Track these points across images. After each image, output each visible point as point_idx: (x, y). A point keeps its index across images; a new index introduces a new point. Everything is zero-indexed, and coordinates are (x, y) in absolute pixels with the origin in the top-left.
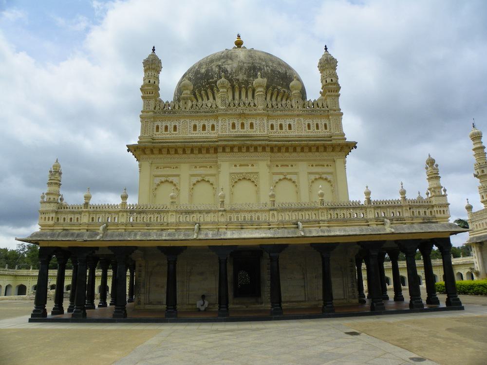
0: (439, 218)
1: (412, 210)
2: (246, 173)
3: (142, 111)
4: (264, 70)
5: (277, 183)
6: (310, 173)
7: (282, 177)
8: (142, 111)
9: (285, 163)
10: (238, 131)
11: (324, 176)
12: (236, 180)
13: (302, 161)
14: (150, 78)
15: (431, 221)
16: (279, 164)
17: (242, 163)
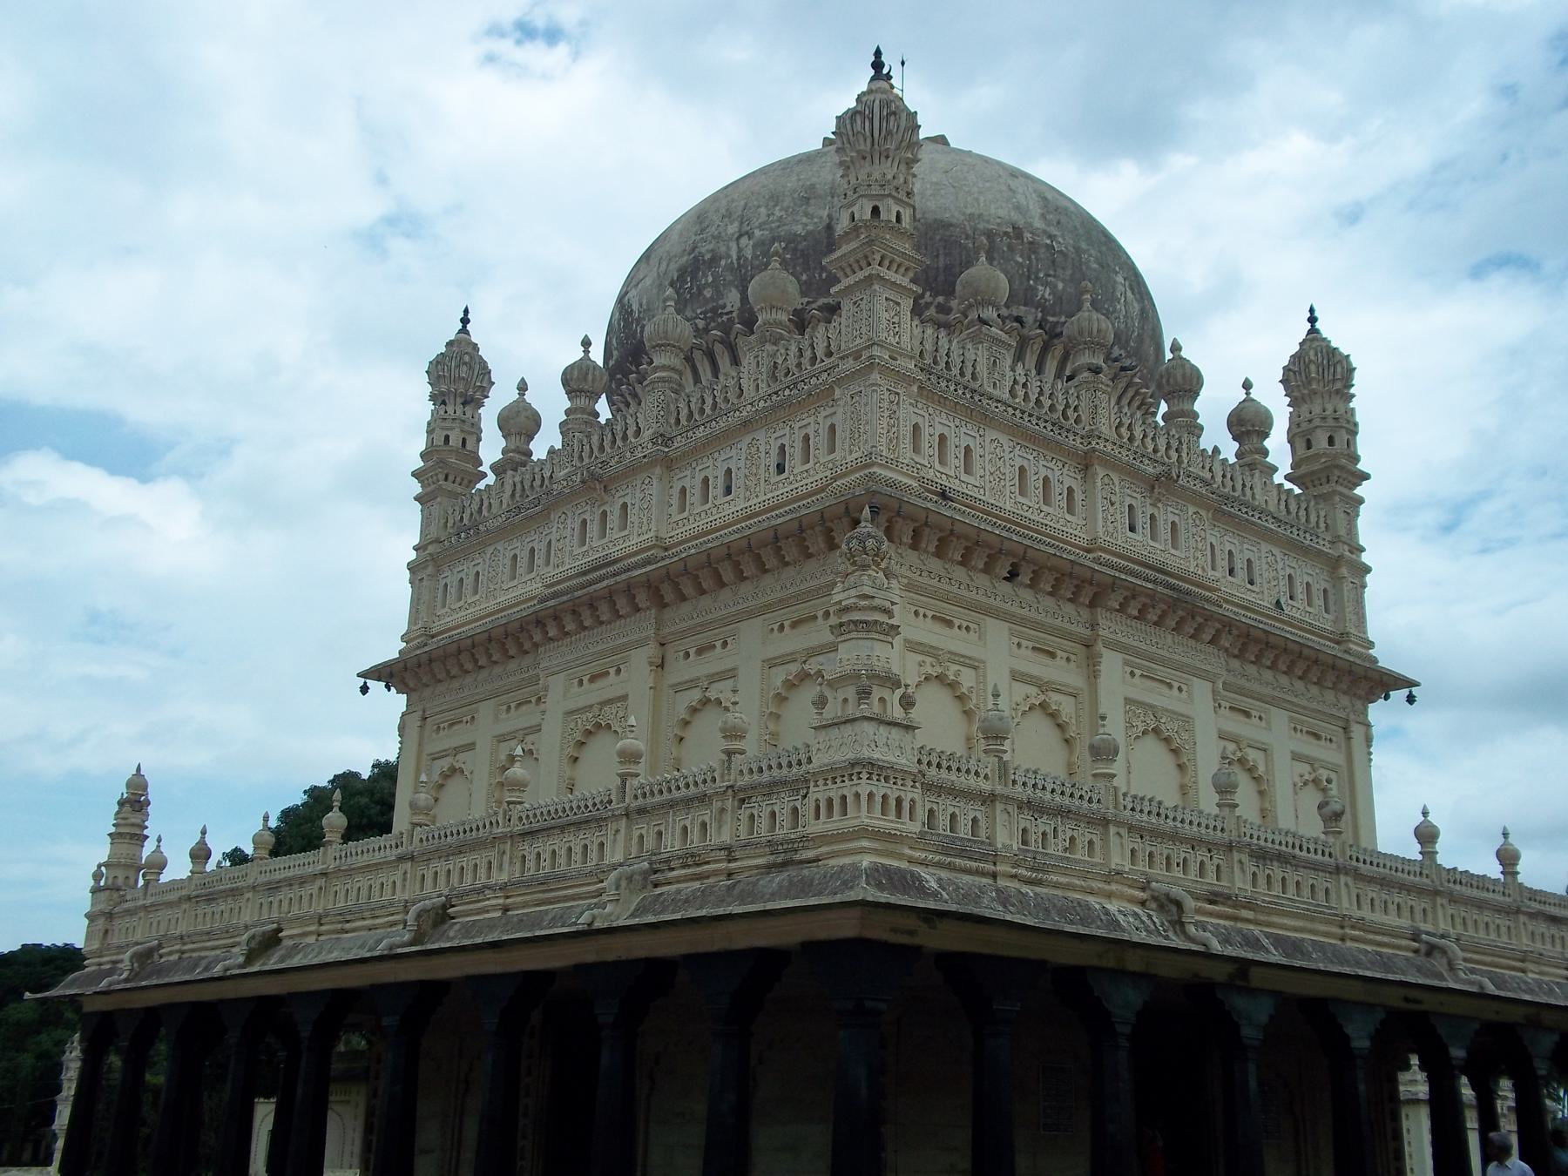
0: (824, 839)
1: (744, 814)
2: (603, 704)
3: (416, 548)
4: (729, 256)
5: (686, 723)
6: (771, 663)
7: (695, 695)
8: (416, 548)
9: (702, 639)
10: (600, 547)
11: (812, 666)
12: (578, 736)
13: (750, 615)
14: (452, 429)
15: (797, 857)
16: (691, 645)
17: (594, 668)
